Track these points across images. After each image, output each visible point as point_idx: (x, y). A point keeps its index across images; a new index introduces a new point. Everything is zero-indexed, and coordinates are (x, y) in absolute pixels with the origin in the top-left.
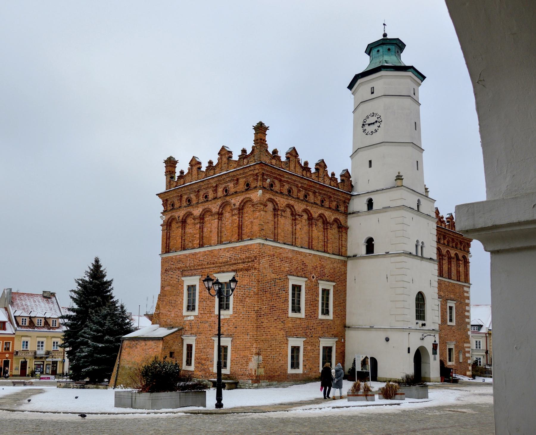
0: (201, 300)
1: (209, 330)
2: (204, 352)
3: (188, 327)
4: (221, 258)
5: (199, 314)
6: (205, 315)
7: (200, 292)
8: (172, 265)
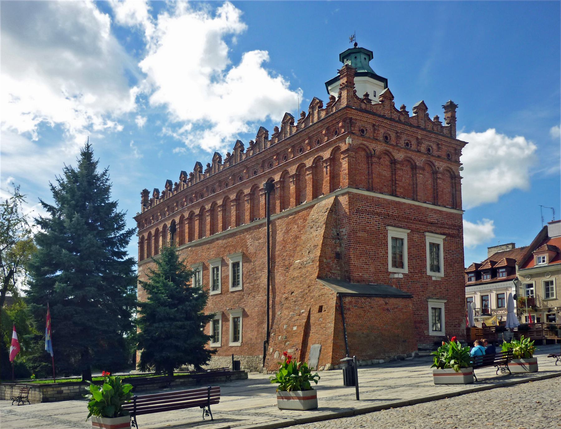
0: (410, 257)
1: (422, 291)
2: (417, 314)
3: (396, 286)
4: (429, 217)
5: (409, 272)
6: (416, 275)
7: (409, 249)
8: (367, 206)
